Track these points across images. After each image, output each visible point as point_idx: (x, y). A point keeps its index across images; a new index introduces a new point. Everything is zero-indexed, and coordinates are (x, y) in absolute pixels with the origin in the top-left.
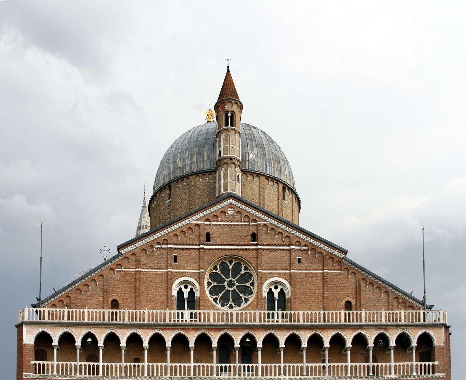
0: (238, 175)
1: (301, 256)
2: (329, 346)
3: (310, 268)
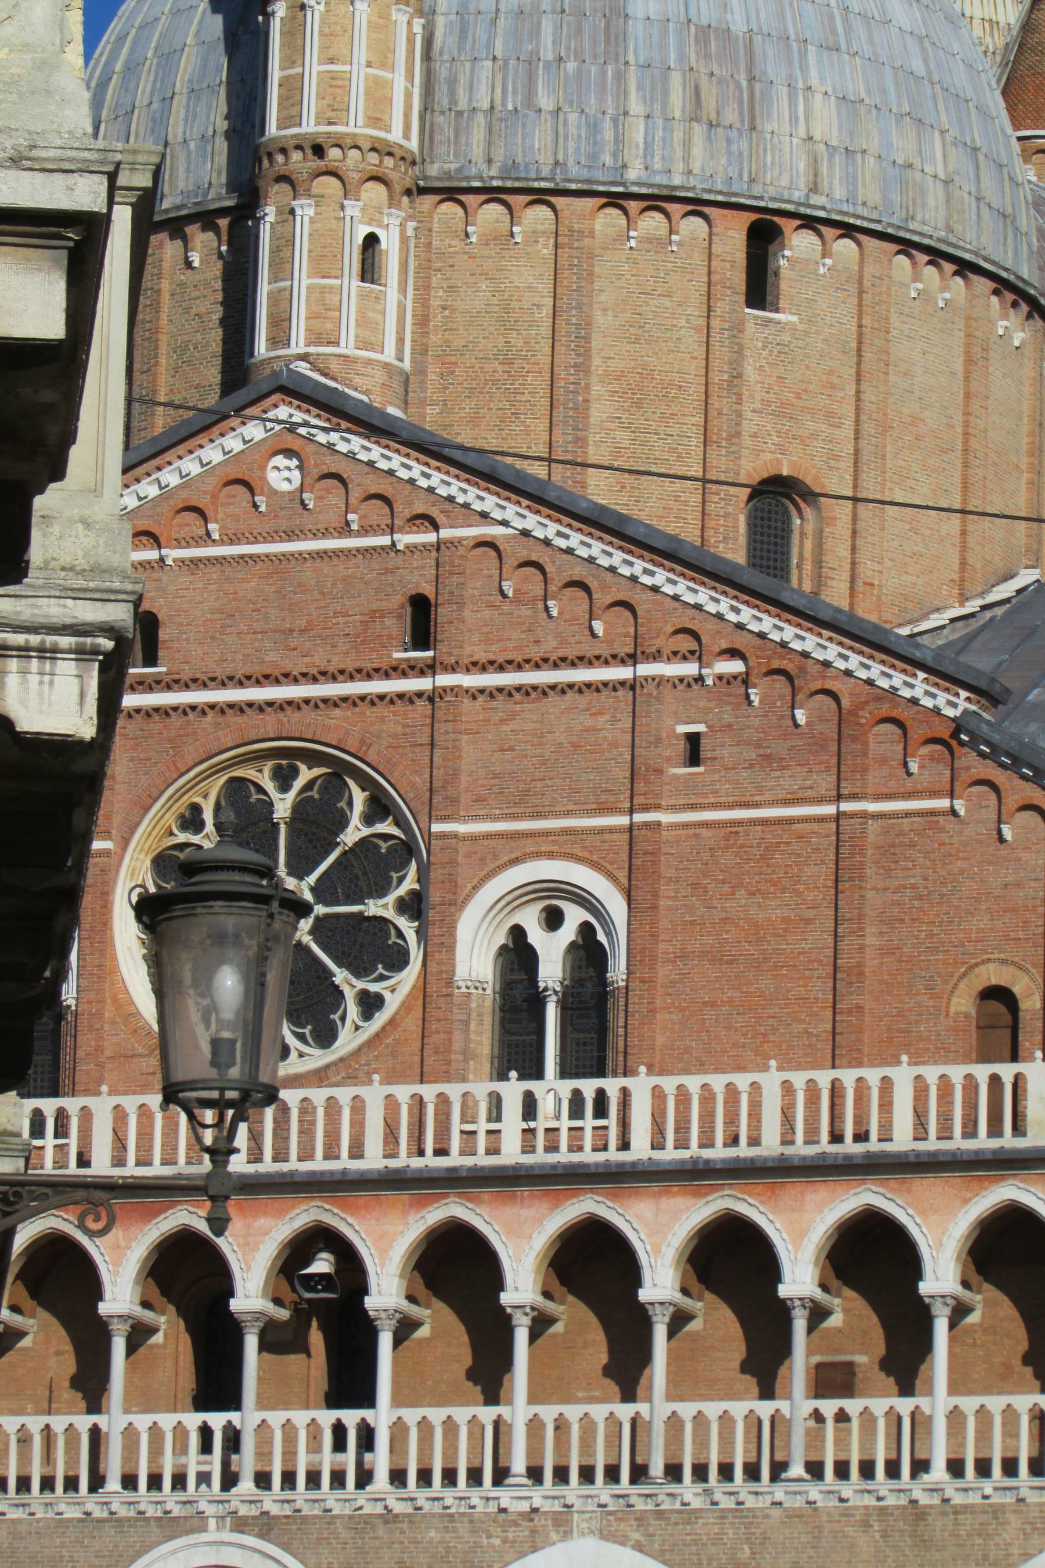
0: (371, 240)
3: (760, 790)
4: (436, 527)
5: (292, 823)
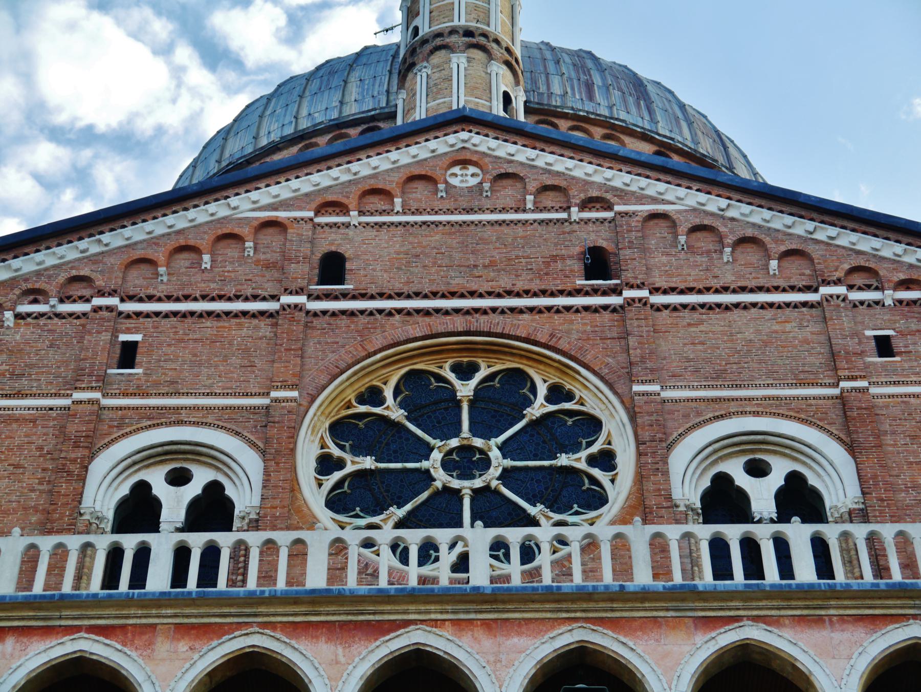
1: (894, 329)
4: (609, 208)
5: (472, 403)
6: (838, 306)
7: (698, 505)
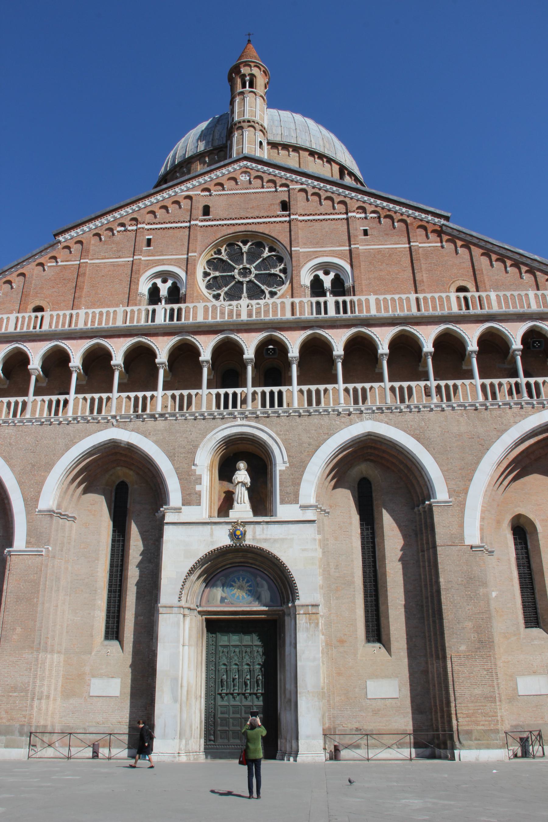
0: (261, 143)
2: (432, 350)
3: (386, 241)
6: (353, 220)
7: (309, 285)
